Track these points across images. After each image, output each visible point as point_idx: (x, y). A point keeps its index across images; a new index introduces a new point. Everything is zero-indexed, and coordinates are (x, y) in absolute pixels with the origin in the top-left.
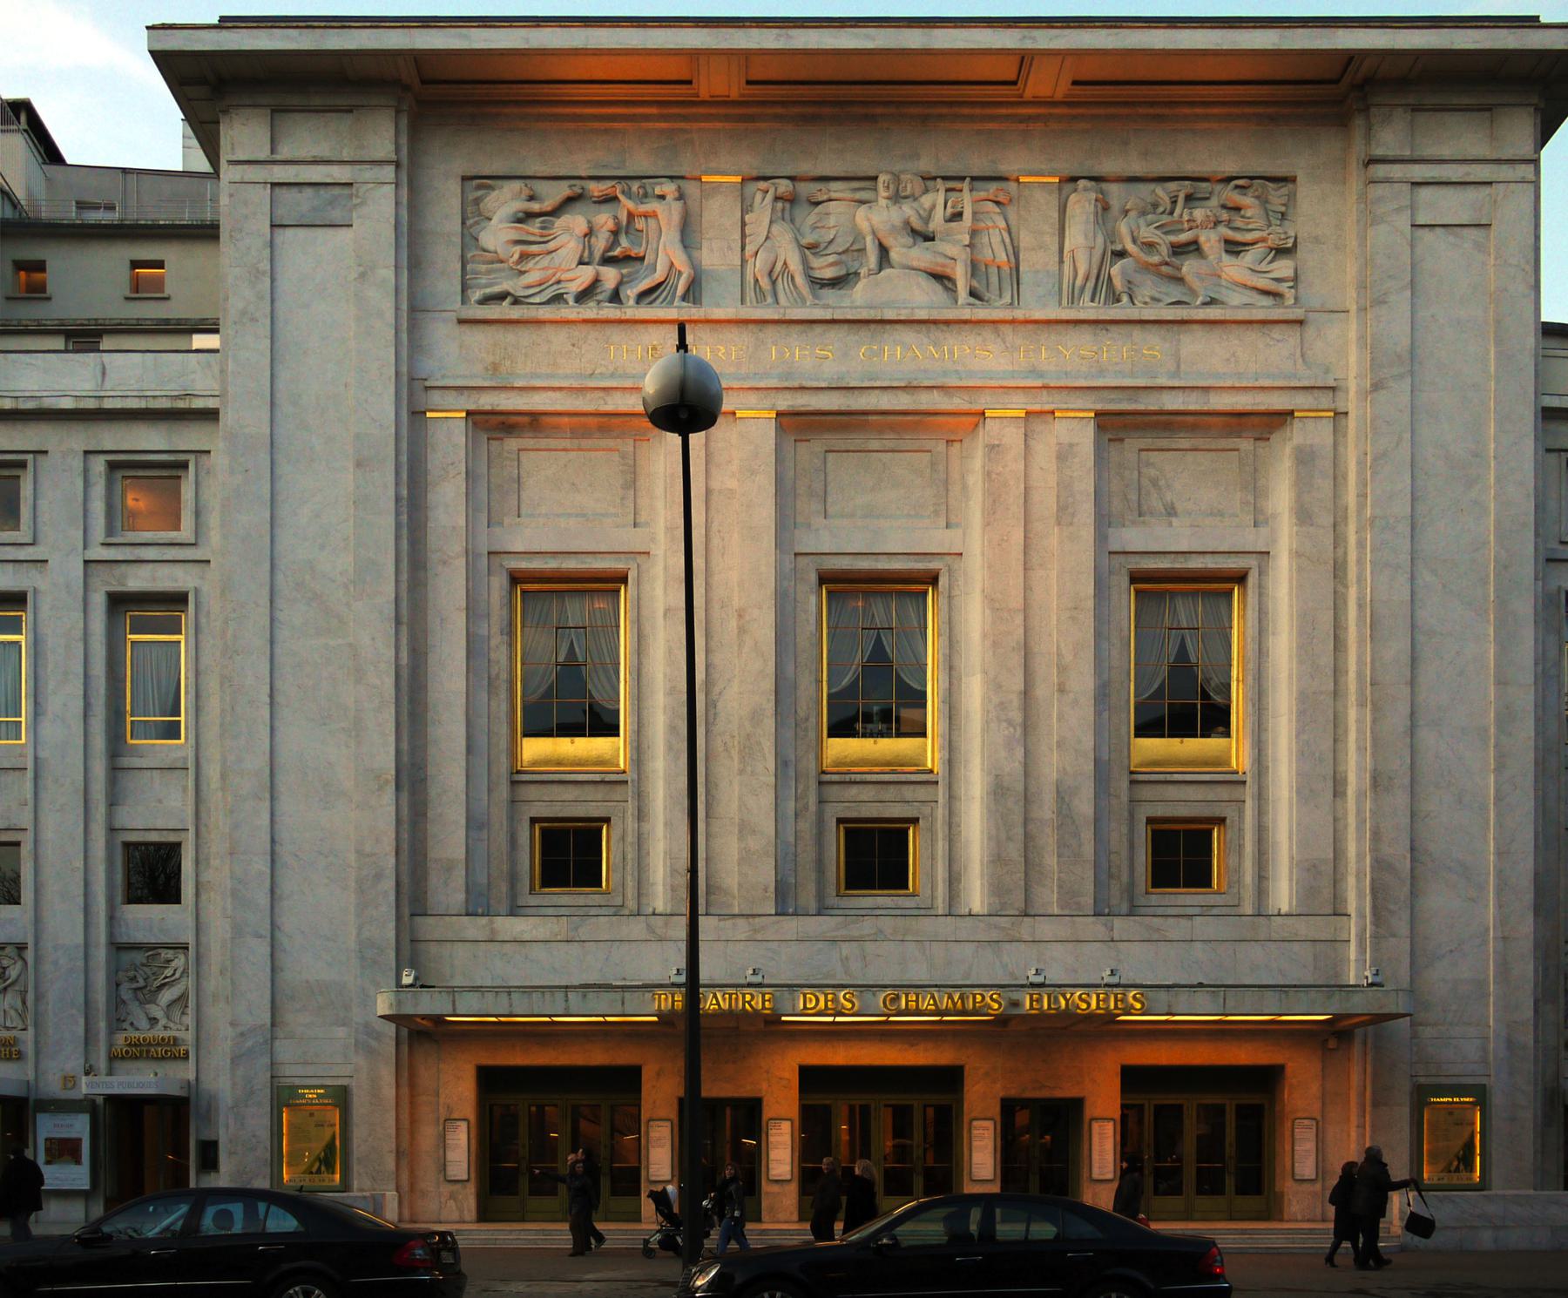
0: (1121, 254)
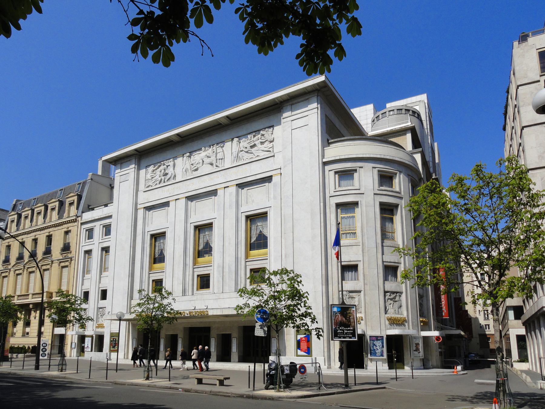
0: (242, 151)
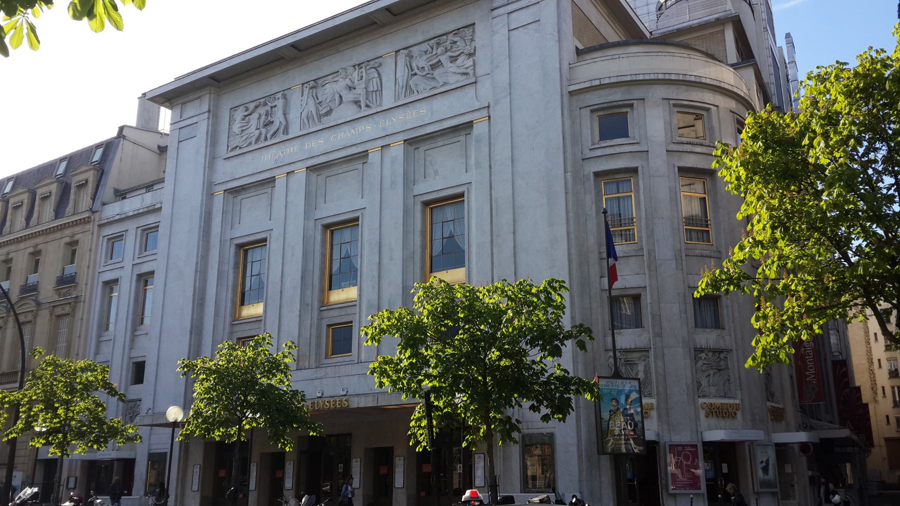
0: (416, 74)
